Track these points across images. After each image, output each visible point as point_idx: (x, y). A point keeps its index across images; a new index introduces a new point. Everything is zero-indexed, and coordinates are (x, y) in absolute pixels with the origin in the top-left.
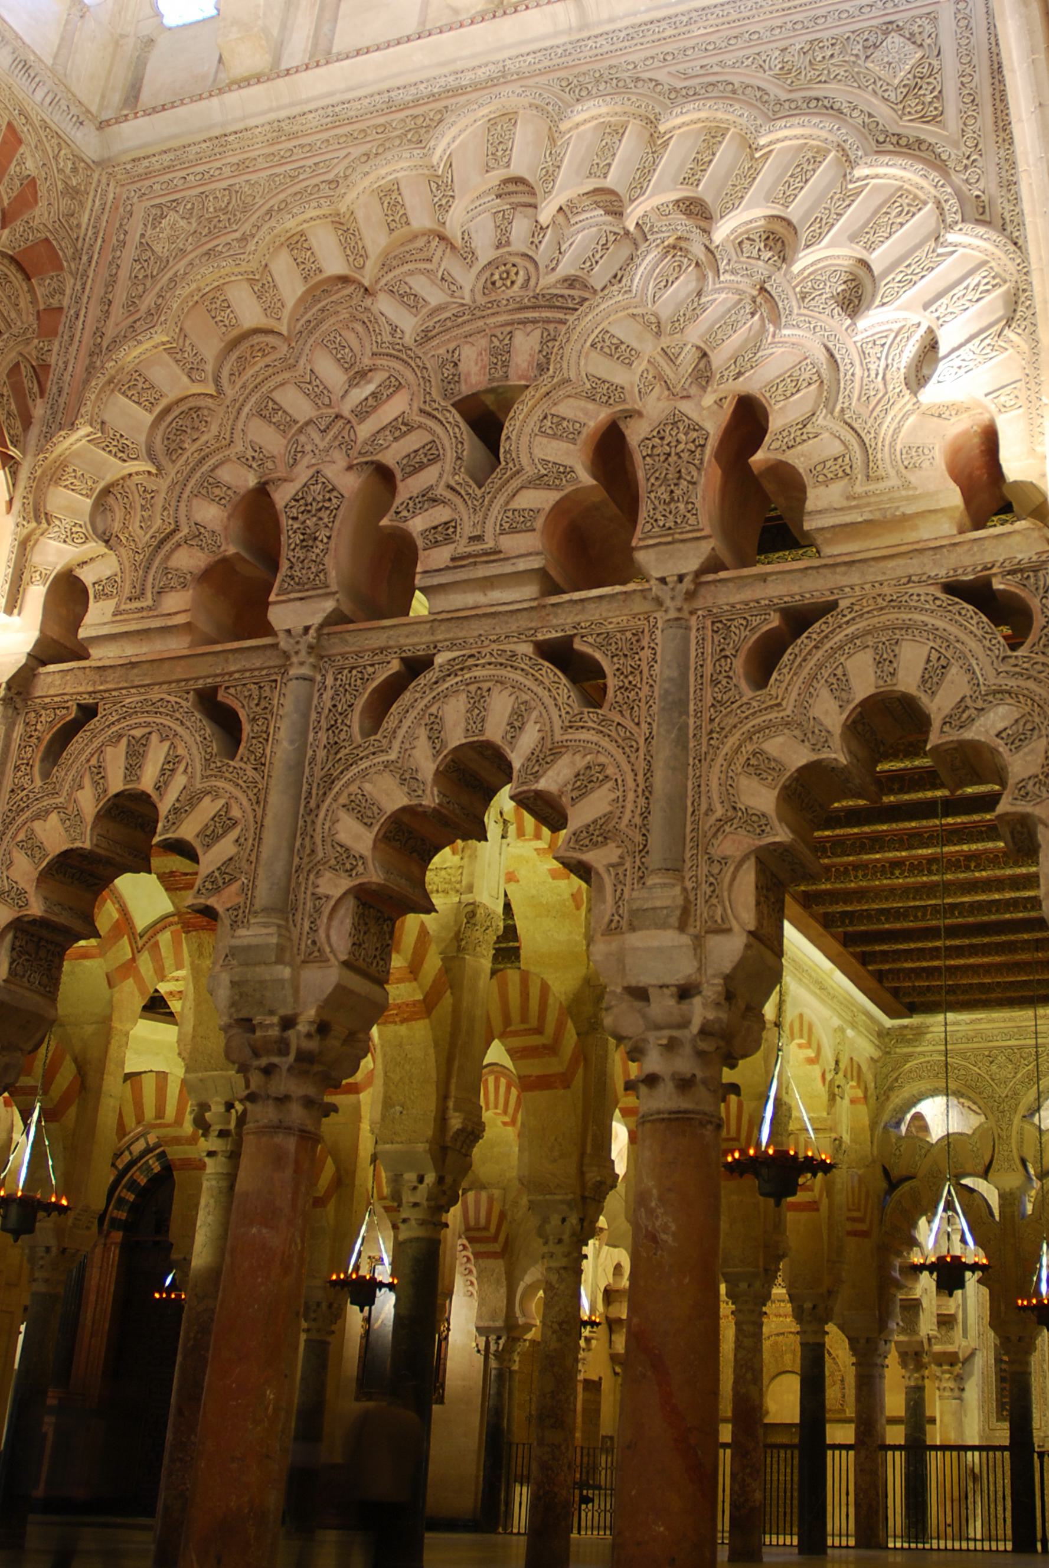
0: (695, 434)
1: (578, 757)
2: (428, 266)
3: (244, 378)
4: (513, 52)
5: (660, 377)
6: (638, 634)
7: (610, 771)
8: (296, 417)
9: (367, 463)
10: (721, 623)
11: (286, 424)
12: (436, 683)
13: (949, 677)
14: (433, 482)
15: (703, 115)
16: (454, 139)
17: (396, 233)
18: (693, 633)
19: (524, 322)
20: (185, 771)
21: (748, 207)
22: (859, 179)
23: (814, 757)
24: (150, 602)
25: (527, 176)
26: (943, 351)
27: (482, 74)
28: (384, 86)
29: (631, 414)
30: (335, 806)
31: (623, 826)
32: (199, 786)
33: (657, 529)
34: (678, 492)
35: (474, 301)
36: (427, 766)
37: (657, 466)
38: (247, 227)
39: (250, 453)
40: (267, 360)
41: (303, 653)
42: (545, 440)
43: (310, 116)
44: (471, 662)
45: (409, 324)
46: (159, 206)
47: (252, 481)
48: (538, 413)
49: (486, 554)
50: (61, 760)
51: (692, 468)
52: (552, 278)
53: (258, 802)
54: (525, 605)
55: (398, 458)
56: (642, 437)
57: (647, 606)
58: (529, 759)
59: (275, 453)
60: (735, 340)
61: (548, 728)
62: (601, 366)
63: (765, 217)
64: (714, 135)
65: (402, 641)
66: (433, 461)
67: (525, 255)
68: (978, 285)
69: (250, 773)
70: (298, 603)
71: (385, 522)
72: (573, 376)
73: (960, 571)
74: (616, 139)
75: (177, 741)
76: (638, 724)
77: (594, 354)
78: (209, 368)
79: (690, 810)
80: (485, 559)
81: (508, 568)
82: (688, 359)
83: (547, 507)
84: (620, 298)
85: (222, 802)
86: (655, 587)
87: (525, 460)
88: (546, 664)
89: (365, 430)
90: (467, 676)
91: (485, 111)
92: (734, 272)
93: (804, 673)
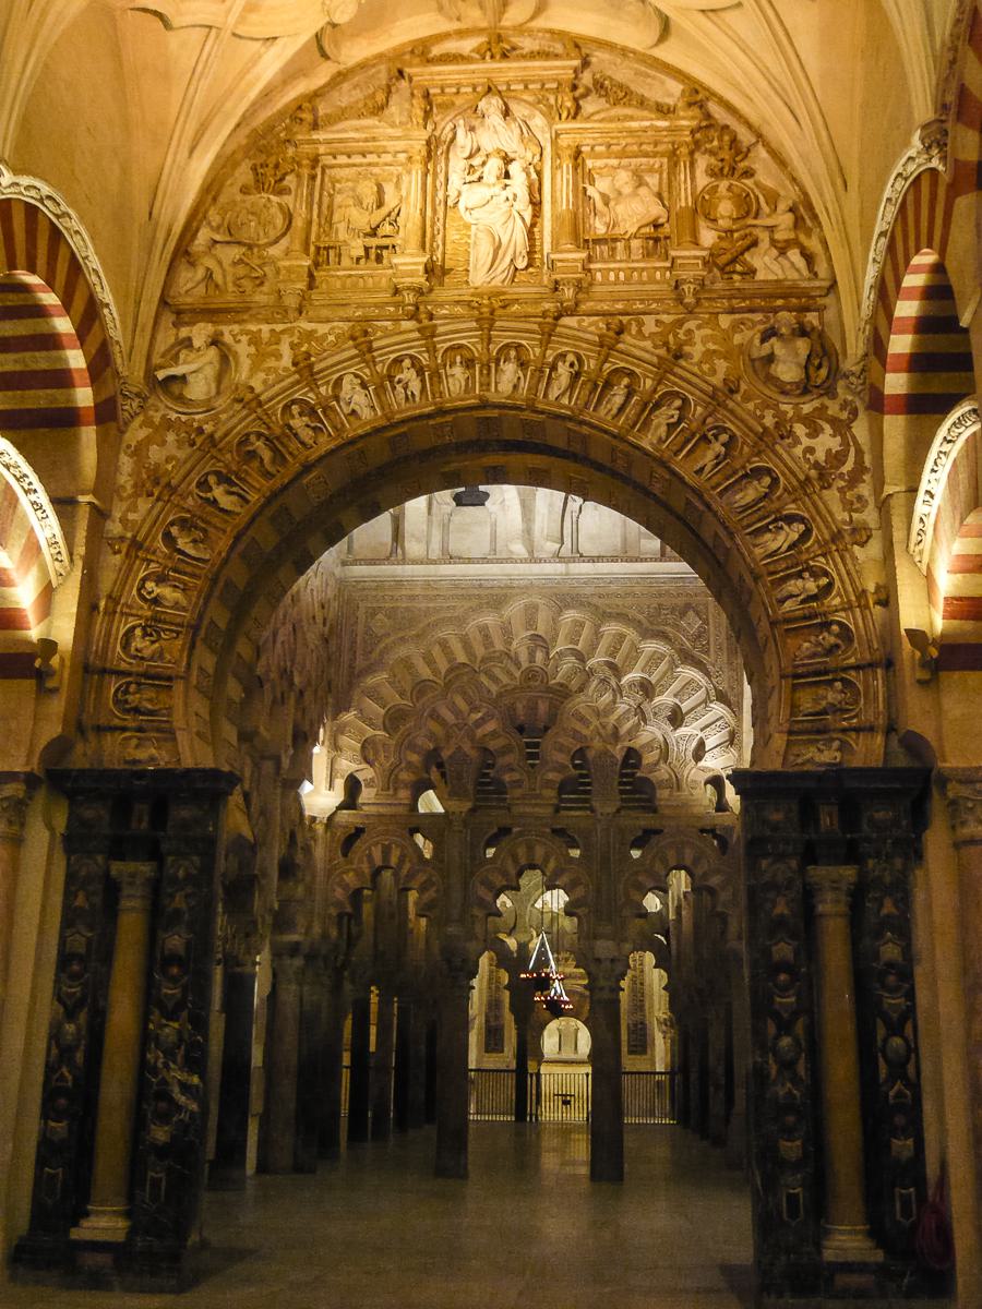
5: (599, 734)
19: (542, 697)
24: (391, 792)
25: (544, 635)
26: (707, 749)
29: (588, 747)
45: (494, 689)
46: (374, 609)
47: (432, 746)
52: (553, 682)
60: (629, 725)
64: (621, 637)
78: (409, 694)
82: (610, 727)
83: (559, 780)
86: (599, 816)
89: (479, 732)
92: (628, 697)
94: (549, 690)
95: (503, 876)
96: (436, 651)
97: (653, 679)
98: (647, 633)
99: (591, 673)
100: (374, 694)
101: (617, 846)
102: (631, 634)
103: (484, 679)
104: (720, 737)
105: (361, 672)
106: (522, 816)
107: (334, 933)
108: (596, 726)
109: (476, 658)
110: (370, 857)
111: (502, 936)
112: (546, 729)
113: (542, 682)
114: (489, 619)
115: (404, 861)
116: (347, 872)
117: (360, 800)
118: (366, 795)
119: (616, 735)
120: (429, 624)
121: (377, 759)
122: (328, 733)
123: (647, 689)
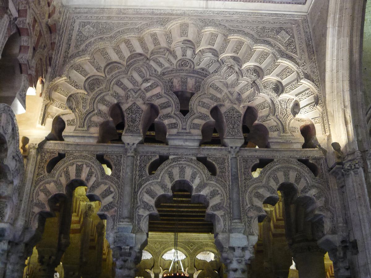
0: (238, 113)
1: (211, 188)
2: (164, 57)
3: (112, 74)
4: (188, 9)
5: (228, 97)
6: (224, 159)
7: (220, 192)
8: (128, 87)
9: (149, 103)
10: (245, 160)
11: (125, 88)
12: (170, 163)
13: (301, 181)
14: (170, 112)
15: (238, 37)
16: (171, 26)
17: (156, 46)
18: (238, 160)
19: (190, 76)
20: (95, 176)
21: (251, 62)
22: (278, 62)
23: (271, 195)
24: (85, 128)
25: (192, 40)
27: (179, 12)
28: (152, 8)
29: (221, 105)
30: (142, 192)
31: (224, 206)
32: (100, 181)
33: (230, 135)
34: (235, 127)
35: (177, 68)
36: (169, 185)
37: (229, 119)
38: (112, 34)
39: (115, 94)
40: (119, 70)
41: (133, 150)
42: (200, 107)
43: (130, 10)
44: (179, 159)
48: (198, 100)
49: (187, 133)
50: (55, 168)
51: (238, 122)
53: (119, 188)
54: (196, 147)
55: (159, 104)
56: (224, 112)
57: (226, 153)
58: (198, 186)
59: (122, 95)
60: (247, 93)
61: (202, 179)
62: (212, 91)
63: (254, 65)
64: (240, 44)
65: (160, 151)
66: (169, 106)
67: (190, 60)
68: (308, 93)
69: (116, 179)
70: (131, 137)
71: (156, 120)
72: (206, 93)
73: (302, 157)
74: (216, 37)
75: (92, 168)
76: (226, 181)
77: (211, 89)
78: (103, 69)
79: (241, 204)
80: (186, 134)
81: (193, 138)
82: (235, 95)
83: (203, 124)
84: (217, 76)
85: (107, 186)
87: (195, 111)
88: (201, 163)
89: (148, 95)
90: (179, 163)
91: (180, 21)
92: (247, 76)
93: (267, 175)
94: (194, 72)
95: (162, 187)
96: (123, 46)
97: (263, 66)
98: (257, 41)
99: (223, 62)
100: (79, 68)
101: (243, 170)
102: (247, 41)
103: (152, 63)
104: (308, 100)
105: (72, 55)
106: (177, 147)
107: (35, 225)
108: (226, 93)
109: (148, 50)
110: (67, 173)
111: (148, 271)
112: (192, 94)
113: (190, 67)
114: (157, 30)
115: (91, 176)
116: (49, 183)
117: (63, 134)
118: (68, 130)
119: (239, 100)
120: (119, 32)
121: (77, 107)
122: (45, 89)
123: (258, 72)
